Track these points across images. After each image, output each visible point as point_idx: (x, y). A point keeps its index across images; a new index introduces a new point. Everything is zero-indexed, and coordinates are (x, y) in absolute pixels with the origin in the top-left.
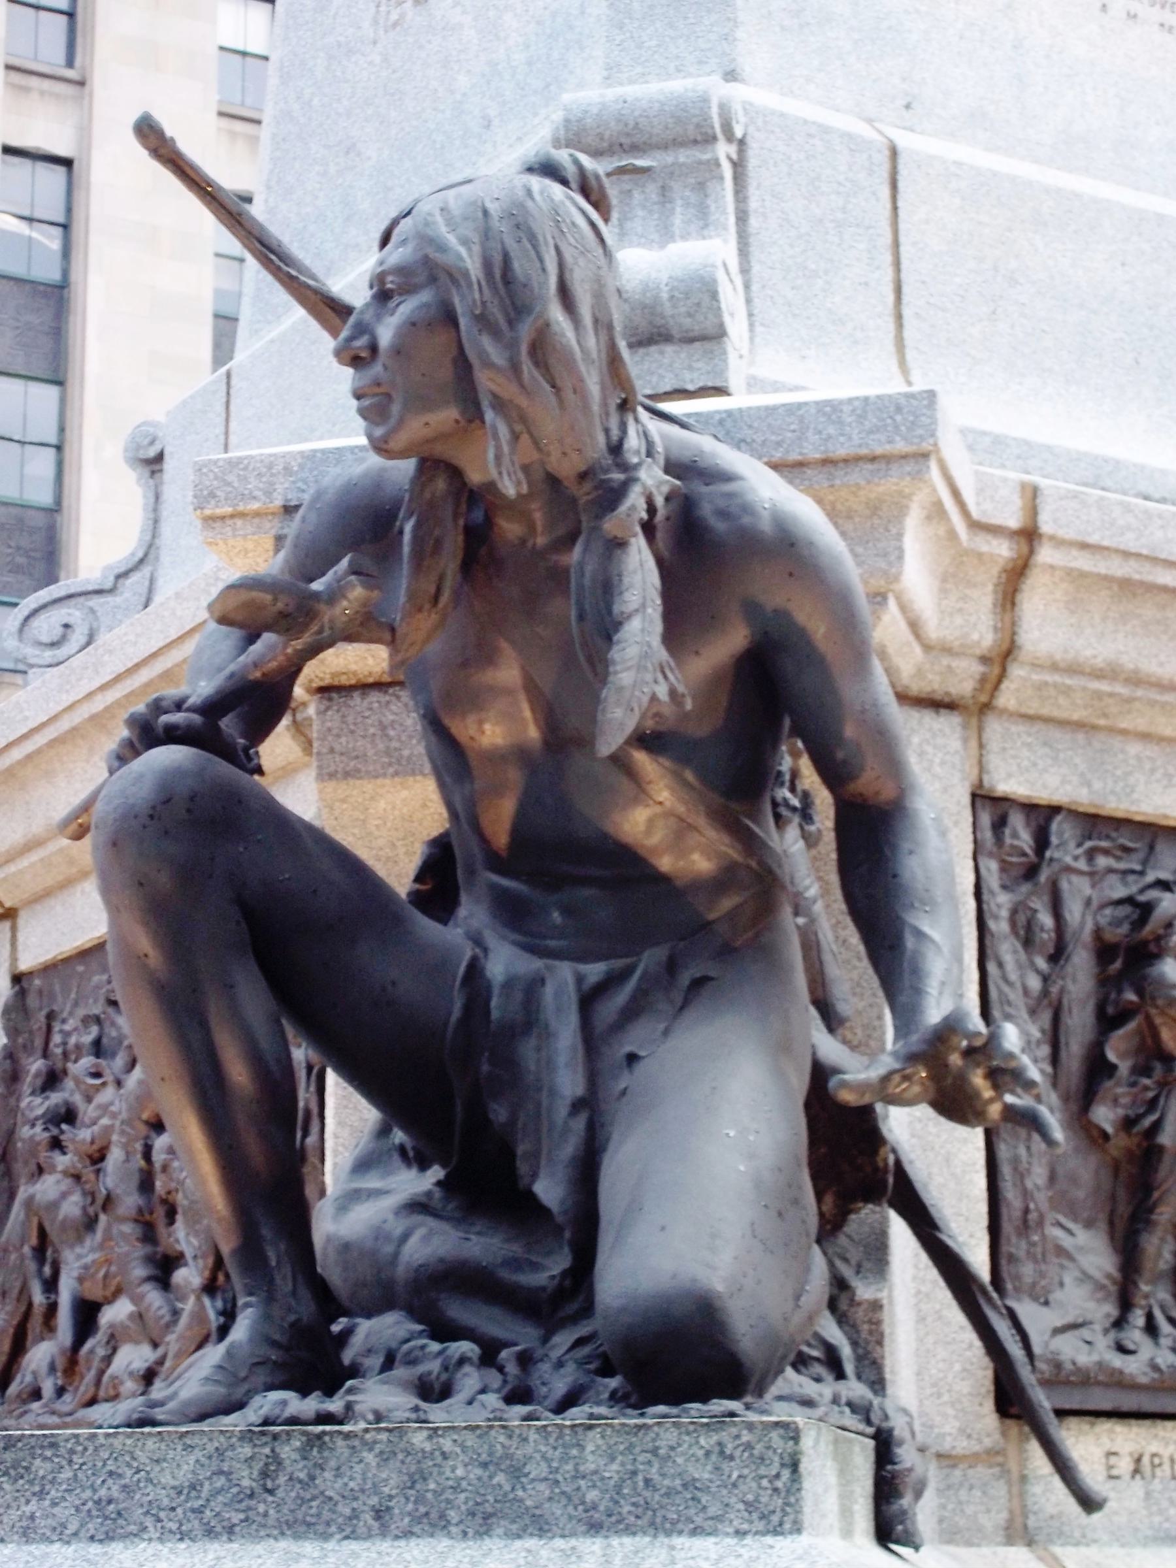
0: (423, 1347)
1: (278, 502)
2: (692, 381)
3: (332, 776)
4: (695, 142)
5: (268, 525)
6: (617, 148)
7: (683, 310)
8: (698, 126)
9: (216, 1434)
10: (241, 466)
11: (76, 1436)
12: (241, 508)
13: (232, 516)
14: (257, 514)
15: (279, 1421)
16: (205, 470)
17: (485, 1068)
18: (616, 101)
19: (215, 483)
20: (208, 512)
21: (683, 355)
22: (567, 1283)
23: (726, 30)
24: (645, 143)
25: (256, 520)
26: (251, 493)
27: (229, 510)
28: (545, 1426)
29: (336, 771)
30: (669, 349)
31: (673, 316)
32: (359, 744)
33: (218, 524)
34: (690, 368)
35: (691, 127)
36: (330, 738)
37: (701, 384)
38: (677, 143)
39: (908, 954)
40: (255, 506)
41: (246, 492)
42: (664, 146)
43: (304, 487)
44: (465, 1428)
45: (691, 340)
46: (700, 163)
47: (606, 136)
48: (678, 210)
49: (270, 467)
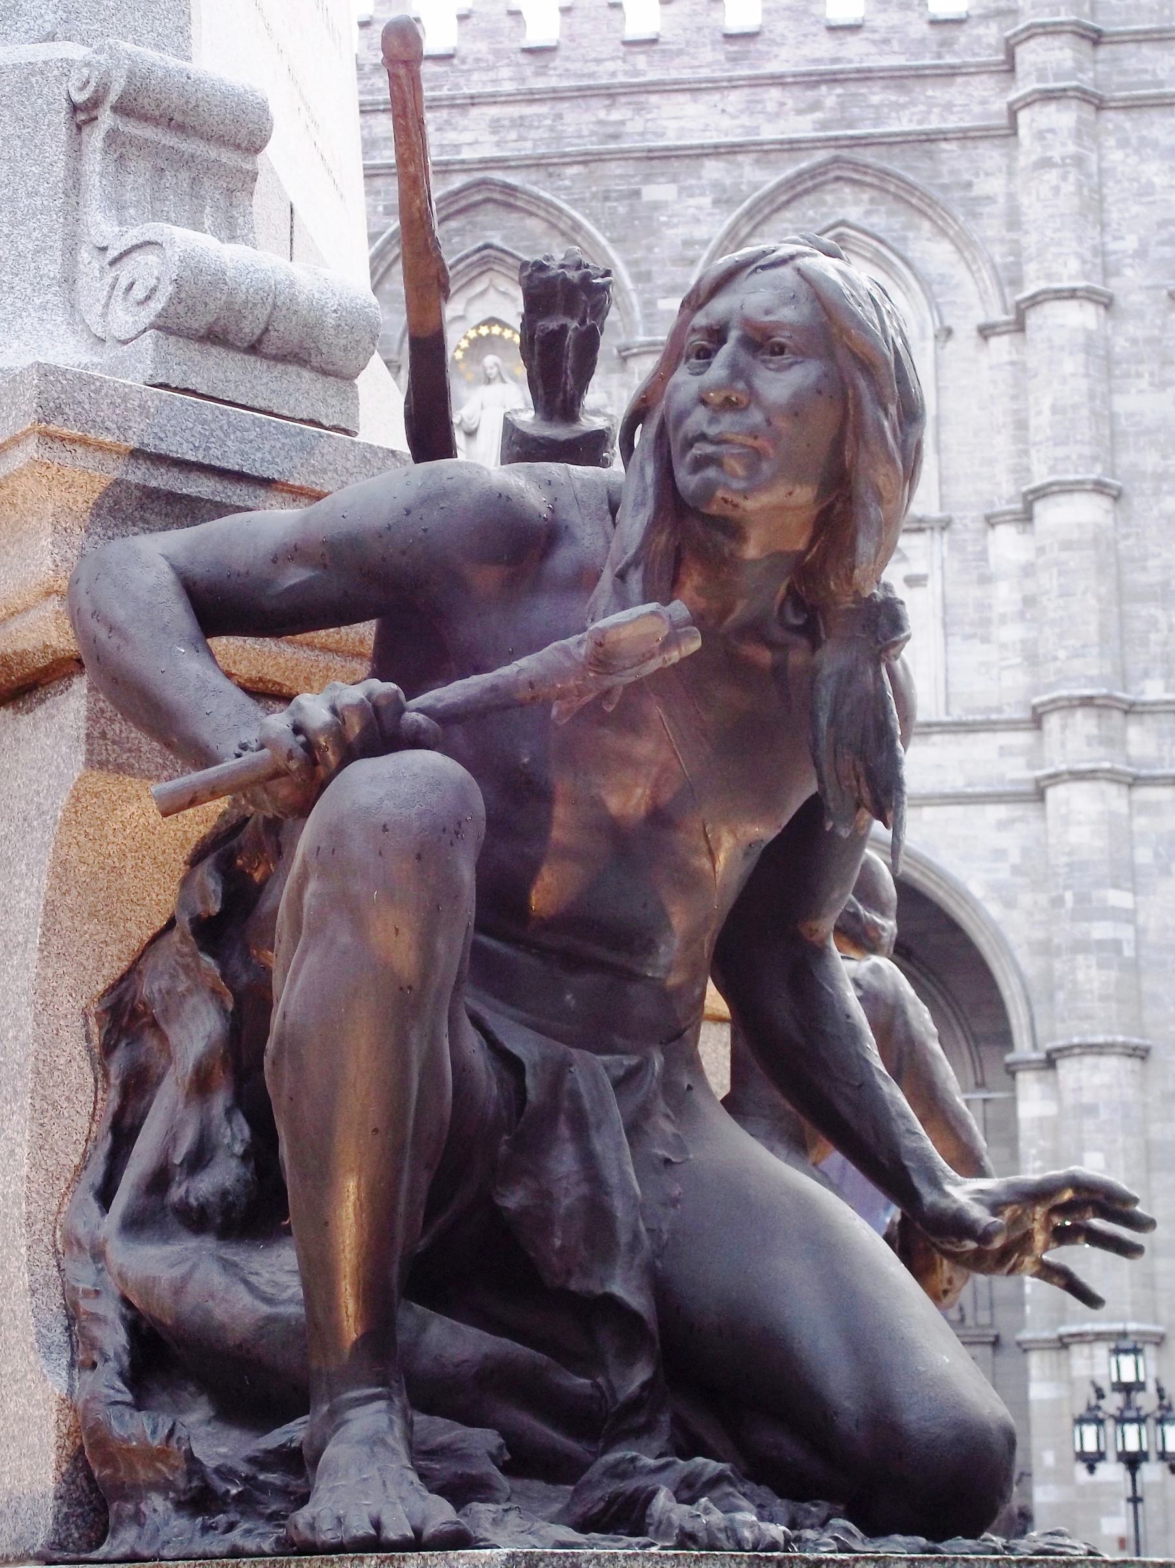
0: (633, 1460)
1: (134, 444)
2: (327, 416)
3: (102, 765)
4: (238, 147)
5: (112, 465)
6: (165, 120)
7: (343, 342)
8: (251, 133)
9: (728, 1559)
10: (93, 387)
11: (597, 1557)
12: (92, 435)
13: (73, 441)
14: (100, 447)
15: (761, 1547)
16: (51, 378)
17: (503, 1149)
18: (180, 72)
19: (63, 396)
20: (52, 428)
21: (319, 386)
22: (646, 1394)
23: (181, 23)
24: (193, 128)
25: (99, 455)
26: (103, 422)
27: (76, 432)
28: (997, 1561)
29: (108, 761)
30: (306, 374)
31: (330, 345)
32: (133, 735)
33: (57, 445)
34: (324, 401)
35: (244, 131)
36: (103, 721)
37: (335, 423)
38: (222, 141)
39: (888, 1098)
40: (109, 439)
41: (99, 419)
42: (208, 139)
43: (163, 435)
44: (936, 1560)
45: (325, 373)
46: (240, 170)
47: (163, 106)
48: (208, 210)
49: (125, 399)
